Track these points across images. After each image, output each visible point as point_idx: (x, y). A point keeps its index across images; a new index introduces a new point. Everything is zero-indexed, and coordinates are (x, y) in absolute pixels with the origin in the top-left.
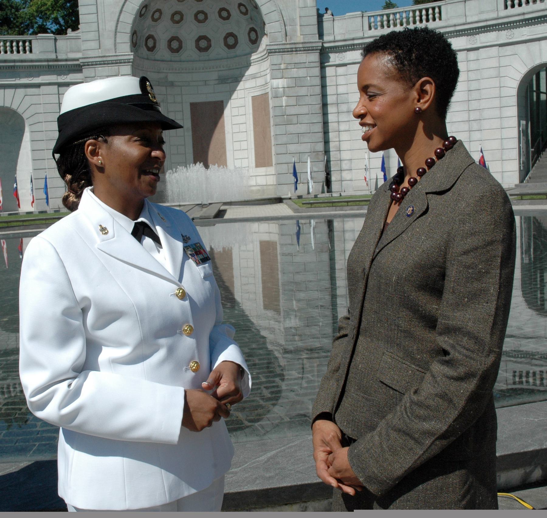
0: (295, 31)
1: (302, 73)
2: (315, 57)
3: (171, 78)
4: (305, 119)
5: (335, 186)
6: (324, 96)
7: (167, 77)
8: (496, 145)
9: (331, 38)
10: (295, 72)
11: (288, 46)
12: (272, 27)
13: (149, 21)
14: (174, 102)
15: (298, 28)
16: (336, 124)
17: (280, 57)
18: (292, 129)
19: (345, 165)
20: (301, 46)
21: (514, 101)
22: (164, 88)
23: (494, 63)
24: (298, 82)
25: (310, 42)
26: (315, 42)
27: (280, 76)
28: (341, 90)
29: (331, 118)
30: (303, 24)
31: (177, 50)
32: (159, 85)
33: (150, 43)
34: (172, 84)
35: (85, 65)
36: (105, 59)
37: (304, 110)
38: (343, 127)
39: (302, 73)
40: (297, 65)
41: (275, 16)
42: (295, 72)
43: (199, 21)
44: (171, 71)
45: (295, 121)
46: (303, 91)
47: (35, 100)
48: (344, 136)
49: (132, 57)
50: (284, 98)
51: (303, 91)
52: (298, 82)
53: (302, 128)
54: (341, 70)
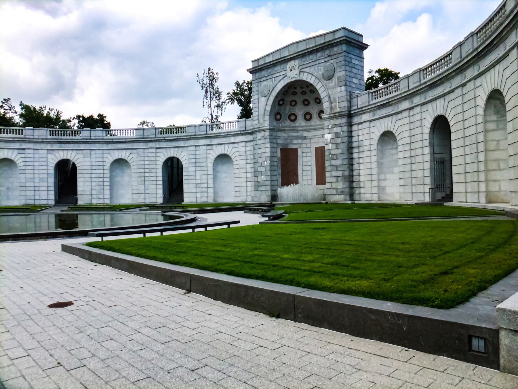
0: (336, 106)
2: (344, 120)
3: (305, 134)
4: (340, 157)
5: (356, 197)
6: (350, 142)
7: (303, 134)
9: (356, 107)
10: (335, 130)
12: (326, 105)
15: (337, 104)
16: (357, 159)
17: (328, 122)
18: (334, 162)
20: (337, 114)
24: (337, 135)
27: (328, 132)
28: (361, 138)
29: (355, 156)
34: (305, 138)
38: (361, 161)
40: (337, 126)
41: (327, 99)
42: (335, 130)
45: (335, 158)
46: (339, 140)
47: (236, 150)
48: (362, 166)
50: (330, 145)
51: (339, 140)
54: (360, 127)
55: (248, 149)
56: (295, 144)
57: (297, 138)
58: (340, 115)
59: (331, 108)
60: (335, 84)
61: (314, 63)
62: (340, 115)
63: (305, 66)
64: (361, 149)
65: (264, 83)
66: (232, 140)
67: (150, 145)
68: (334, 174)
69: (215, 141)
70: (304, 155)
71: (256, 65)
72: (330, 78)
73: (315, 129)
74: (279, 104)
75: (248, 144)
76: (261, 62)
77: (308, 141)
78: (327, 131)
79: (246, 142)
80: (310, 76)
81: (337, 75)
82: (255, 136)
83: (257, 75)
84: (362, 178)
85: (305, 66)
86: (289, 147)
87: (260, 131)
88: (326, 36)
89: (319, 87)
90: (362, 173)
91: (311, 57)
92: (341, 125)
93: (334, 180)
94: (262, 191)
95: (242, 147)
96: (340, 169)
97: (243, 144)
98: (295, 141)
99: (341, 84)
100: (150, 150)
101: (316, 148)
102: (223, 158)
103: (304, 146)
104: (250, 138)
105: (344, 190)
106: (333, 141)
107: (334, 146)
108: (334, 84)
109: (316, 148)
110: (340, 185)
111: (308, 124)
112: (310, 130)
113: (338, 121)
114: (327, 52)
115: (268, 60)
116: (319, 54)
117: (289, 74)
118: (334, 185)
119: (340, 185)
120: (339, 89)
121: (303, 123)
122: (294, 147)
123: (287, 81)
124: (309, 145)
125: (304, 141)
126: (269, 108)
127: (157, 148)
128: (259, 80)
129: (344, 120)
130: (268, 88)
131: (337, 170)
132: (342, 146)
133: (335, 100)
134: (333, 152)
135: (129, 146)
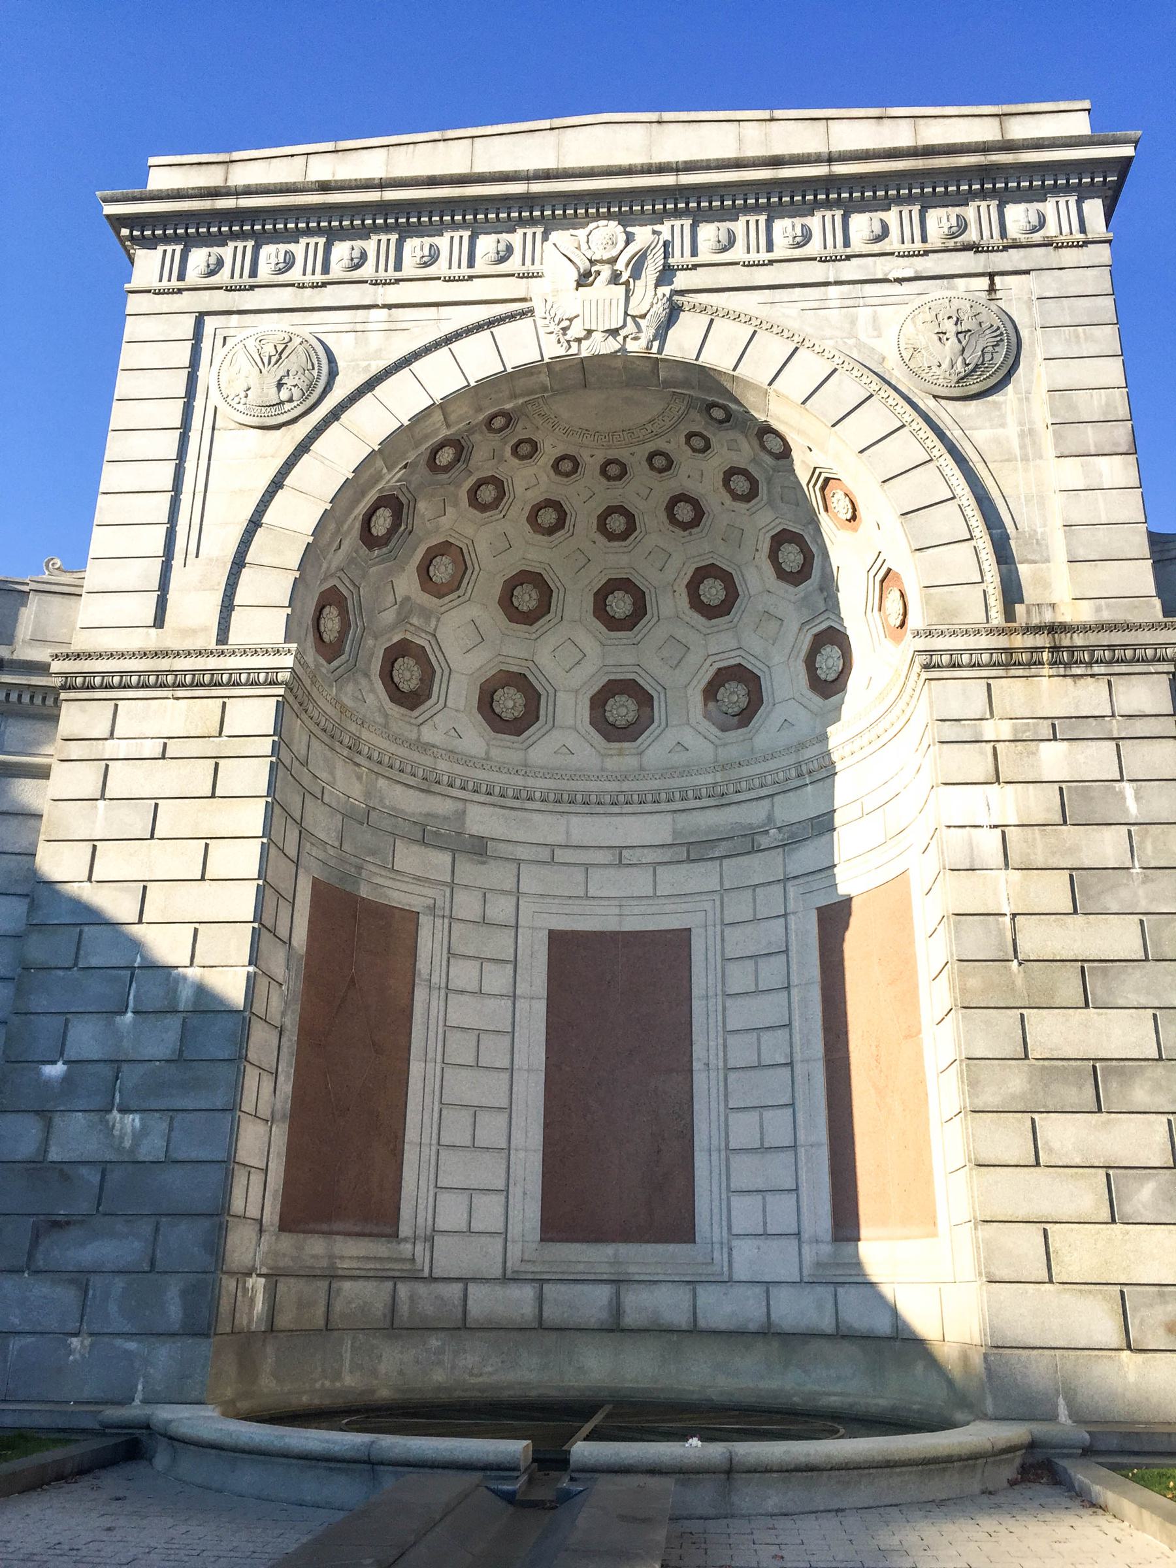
1: (1095, 761)
3: (482, 821)
10: (1055, 760)
11: (1018, 641)
13: (407, 583)
14: (484, 922)
22: (445, 858)
25: (1128, 627)
26: (1153, 626)
30: (1082, 554)
32: (423, 842)
33: (408, 674)
35: (73, 688)
36: (164, 664)
37: (1117, 938)
39: (1095, 761)
43: (611, 536)
44: (482, 798)
46: (1106, 846)
49: (289, 661)
51: (1106, 846)
52: (1074, 805)
53: (1121, 1034)
56: (406, 878)
57: (425, 835)
60: (1028, 434)
61: (818, 272)
68: (1065, 1135)
70: (464, 974)
73: (562, 802)
74: (368, 538)
77: (498, 875)
81: (1036, 374)
86: (364, 892)
92: (1116, 727)
94: (81, 1279)
96: (1140, 1095)
98: (409, 858)
99: (1091, 437)
101: (557, 940)
103: (467, 905)
106: (1038, 847)
108: (1011, 432)
109: (557, 940)
112: (524, 797)
118: (1080, 1252)
120: (1072, 472)
121: (474, 737)
122: (399, 896)
125: (468, 871)
126: (298, 515)
134: (1037, 940)
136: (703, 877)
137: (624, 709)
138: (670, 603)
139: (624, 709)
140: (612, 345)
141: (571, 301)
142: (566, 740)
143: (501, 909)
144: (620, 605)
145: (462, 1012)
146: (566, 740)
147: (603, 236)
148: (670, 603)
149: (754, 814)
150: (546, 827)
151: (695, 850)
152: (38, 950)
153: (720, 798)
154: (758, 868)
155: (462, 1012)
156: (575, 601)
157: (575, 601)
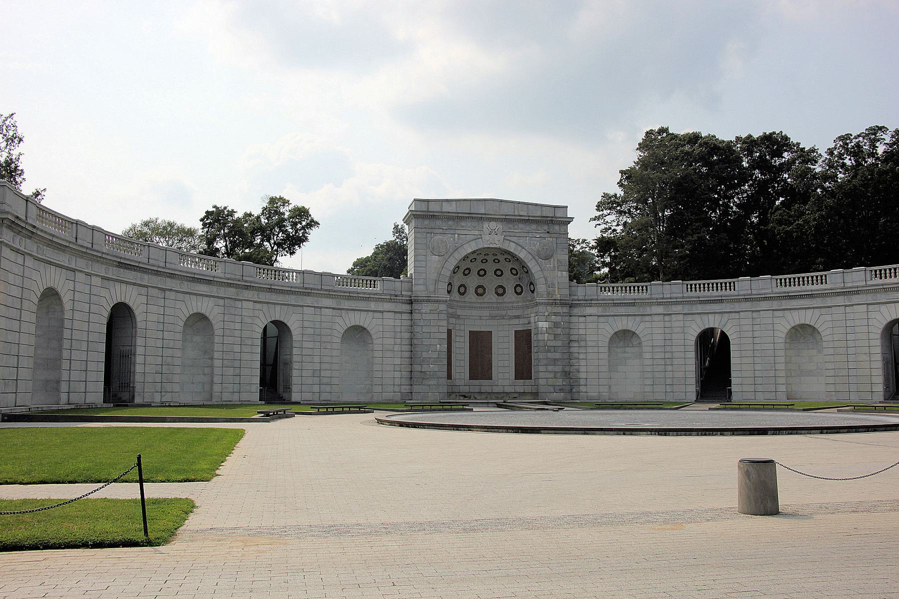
0: (554, 291)
1: (558, 319)
3: (459, 312)
8: (681, 375)
12: (541, 288)
18: (550, 355)
19: (582, 382)
21: (693, 348)
23: (681, 324)
24: (556, 325)
31: (463, 294)
34: (458, 317)
37: (559, 343)
39: (558, 319)
40: (556, 314)
45: (553, 350)
46: (559, 331)
51: (559, 331)
52: (556, 325)
53: (557, 356)
55: (398, 323)
58: (563, 303)
59: (548, 294)
62: (563, 303)
63: (511, 234)
64: (583, 344)
65: (439, 237)
66: (373, 306)
67: (247, 294)
68: (550, 368)
69: (346, 304)
71: (424, 207)
72: (547, 258)
73: (471, 308)
75: (399, 315)
76: (433, 208)
78: (544, 318)
79: (395, 312)
80: (520, 248)
82: (415, 306)
83: (426, 222)
84: (583, 375)
85: (511, 234)
87: (429, 301)
88: (544, 209)
89: (532, 265)
90: (582, 369)
91: (521, 226)
93: (552, 375)
95: (390, 321)
97: (391, 315)
100: (245, 304)
102: (357, 333)
103: (458, 327)
104: (407, 307)
105: (564, 387)
107: (552, 337)
110: (560, 382)
111: (462, 298)
113: (559, 309)
114: (546, 227)
115: (446, 208)
116: (534, 226)
117: (486, 237)
118: (551, 382)
119: (560, 382)
123: (481, 245)
124: (462, 327)
127: (255, 302)
128: (430, 231)
129: (565, 310)
130: (446, 246)
131: (554, 365)
132: (561, 337)
133: (553, 285)
134: (550, 343)
135: (214, 290)
136: (495, 322)
137: (480, 291)
138: (490, 273)
139: (480, 291)
140: (494, 246)
141: (487, 237)
142: (471, 296)
143: (462, 327)
144: (482, 273)
145: (458, 345)
146: (471, 296)
147: (493, 225)
148: (490, 273)
149: (504, 313)
150: (467, 312)
151: (493, 317)
152: (415, 341)
153: (498, 309)
154: (503, 322)
155: (458, 345)
156: (474, 272)
157: (474, 272)
